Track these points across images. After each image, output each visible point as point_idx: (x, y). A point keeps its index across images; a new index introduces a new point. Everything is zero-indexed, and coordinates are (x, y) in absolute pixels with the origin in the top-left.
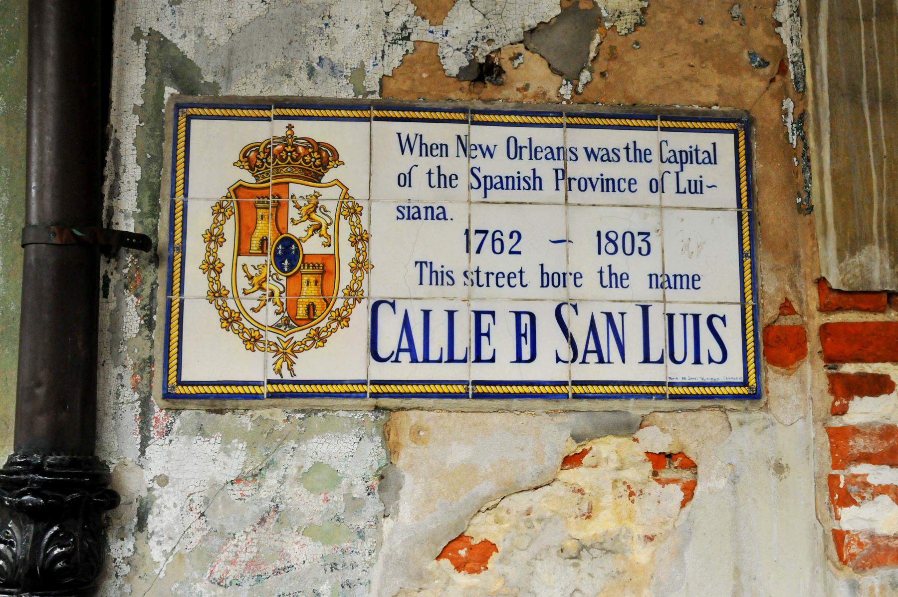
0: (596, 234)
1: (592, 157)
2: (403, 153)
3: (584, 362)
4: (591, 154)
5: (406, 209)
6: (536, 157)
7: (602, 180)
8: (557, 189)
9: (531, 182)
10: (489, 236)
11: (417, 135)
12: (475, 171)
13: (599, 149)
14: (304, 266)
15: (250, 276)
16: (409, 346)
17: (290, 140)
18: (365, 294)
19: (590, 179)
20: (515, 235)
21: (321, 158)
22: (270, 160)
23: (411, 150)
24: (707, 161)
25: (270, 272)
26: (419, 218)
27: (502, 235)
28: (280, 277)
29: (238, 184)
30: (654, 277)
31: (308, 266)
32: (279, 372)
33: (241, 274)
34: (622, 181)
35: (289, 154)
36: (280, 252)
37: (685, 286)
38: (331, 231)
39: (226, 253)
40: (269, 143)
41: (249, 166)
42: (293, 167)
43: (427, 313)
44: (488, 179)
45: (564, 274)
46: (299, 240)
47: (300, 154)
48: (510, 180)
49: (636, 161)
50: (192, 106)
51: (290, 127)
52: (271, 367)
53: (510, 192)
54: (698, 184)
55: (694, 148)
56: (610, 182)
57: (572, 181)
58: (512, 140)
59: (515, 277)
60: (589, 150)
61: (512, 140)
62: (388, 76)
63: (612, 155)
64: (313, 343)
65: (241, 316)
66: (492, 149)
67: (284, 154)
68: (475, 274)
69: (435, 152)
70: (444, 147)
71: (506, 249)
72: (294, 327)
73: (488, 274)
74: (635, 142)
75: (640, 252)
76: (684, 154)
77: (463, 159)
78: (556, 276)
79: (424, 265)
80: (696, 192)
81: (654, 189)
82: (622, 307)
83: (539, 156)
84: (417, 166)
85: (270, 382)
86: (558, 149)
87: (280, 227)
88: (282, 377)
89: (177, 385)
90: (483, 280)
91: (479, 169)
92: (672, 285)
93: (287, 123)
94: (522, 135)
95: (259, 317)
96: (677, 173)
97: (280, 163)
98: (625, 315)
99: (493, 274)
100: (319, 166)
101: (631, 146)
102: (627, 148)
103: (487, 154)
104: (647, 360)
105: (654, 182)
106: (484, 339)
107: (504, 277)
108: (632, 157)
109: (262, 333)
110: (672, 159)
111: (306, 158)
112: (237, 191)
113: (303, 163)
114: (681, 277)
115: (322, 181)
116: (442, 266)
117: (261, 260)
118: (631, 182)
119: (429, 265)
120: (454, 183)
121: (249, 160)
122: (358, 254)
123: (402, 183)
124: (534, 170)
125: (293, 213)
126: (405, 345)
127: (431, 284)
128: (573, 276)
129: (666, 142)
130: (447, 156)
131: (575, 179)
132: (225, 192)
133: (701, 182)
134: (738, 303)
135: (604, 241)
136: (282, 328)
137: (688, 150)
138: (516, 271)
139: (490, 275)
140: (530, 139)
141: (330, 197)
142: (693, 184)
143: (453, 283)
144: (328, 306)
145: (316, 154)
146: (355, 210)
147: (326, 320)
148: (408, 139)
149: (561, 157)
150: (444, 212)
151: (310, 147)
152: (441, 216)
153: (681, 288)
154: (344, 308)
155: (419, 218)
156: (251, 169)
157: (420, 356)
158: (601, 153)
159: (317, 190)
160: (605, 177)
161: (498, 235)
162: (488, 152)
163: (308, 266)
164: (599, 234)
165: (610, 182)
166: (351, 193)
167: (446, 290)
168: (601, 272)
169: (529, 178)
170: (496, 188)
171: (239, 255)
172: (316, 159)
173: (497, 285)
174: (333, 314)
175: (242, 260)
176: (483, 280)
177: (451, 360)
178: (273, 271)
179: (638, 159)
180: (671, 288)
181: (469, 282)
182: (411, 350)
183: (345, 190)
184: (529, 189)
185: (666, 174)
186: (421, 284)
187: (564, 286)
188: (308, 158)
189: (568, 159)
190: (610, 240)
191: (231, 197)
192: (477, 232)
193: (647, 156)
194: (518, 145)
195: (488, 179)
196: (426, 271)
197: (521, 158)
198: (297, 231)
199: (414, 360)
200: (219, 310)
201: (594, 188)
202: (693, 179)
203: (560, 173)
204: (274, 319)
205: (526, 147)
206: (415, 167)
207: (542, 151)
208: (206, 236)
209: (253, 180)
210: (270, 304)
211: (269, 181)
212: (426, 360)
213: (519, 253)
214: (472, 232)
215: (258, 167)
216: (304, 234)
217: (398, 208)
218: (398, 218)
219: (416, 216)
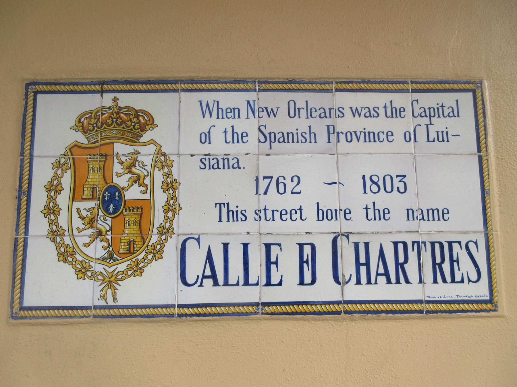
0: (362, 177)
1: (357, 115)
2: (204, 117)
4: (356, 112)
5: (207, 160)
7: (365, 133)
8: (329, 142)
9: (307, 136)
12: (262, 128)
13: (362, 108)
14: (126, 210)
15: (82, 217)
19: (355, 132)
20: (296, 179)
22: (99, 124)
23: (211, 114)
24: (451, 114)
27: (285, 179)
28: (107, 218)
30: (410, 212)
31: (129, 209)
34: (381, 134)
36: (107, 198)
44: (273, 135)
46: (122, 189)
48: (290, 135)
49: (392, 117)
51: (115, 100)
52: (98, 294)
55: (440, 105)
56: (372, 135)
57: (341, 135)
58: (292, 104)
59: (296, 213)
60: (354, 110)
61: (292, 104)
63: (372, 112)
67: (110, 121)
68: (263, 212)
69: (229, 115)
70: (236, 111)
71: (289, 190)
72: (118, 260)
73: (273, 211)
74: (391, 102)
75: (399, 191)
76: (432, 110)
78: (329, 212)
79: (222, 205)
80: (443, 141)
81: (408, 139)
83: (314, 114)
84: (214, 126)
90: (269, 215)
91: (265, 127)
93: (112, 95)
94: (300, 98)
95: (89, 251)
96: (427, 126)
97: (107, 127)
99: (277, 211)
100: (138, 129)
101: (389, 105)
102: (385, 107)
105: (407, 134)
108: (389, 113)
109: (92, 264)
110: (423, 114)
112: (72, 150)
113: (125, 127)
114: (433, 210)
116: (237, 207)
117: (91, 204)
118: (389, 134)
119: (226, 205)
120: (245, 139)
123: (203, 141)
124: (310, 127)
125: (117, 168)
127: (228, 221)
129: (417, 101)
130: (239, 117)
131: (343, 133)
133: (447, 132)
135: (368, 183)
136: (108, 261)
137: (436, 106)
139: (275, 212)
147: (144, 253)
148: (208, 105)
154: (158, 242)
155: (218, 168)
156: (85, 131)
158: (364, 112)
159: (136, 148)
160: (367, 131)
161: (281, 180)
162: (272, 113)
163: (129, 209)
164: (364, 177)
165: (372, 135)
166: (164, 150)
168: (366, 208)
169: (306, 134)
170: (279, 142)
171: (73, 200)
173: (281, 219)
174: (150, 248)
176: (269, 215)
178: (101, 213)
185: (418, 128)
186: (220, 220)
187: (336, 219)
192: (265, 178)
194: (297, 107)
195: (273, 135)
196: (224, 210)
197: (299, 117)
198: (121, 181)
201: (358, 140)
202: (440, 131)
203: (331, 128)
204: (101, 253)
205: (304, 109)
206: (213, 127)
207: (316, 111)
209: (86, 142)
218: (200, 168)
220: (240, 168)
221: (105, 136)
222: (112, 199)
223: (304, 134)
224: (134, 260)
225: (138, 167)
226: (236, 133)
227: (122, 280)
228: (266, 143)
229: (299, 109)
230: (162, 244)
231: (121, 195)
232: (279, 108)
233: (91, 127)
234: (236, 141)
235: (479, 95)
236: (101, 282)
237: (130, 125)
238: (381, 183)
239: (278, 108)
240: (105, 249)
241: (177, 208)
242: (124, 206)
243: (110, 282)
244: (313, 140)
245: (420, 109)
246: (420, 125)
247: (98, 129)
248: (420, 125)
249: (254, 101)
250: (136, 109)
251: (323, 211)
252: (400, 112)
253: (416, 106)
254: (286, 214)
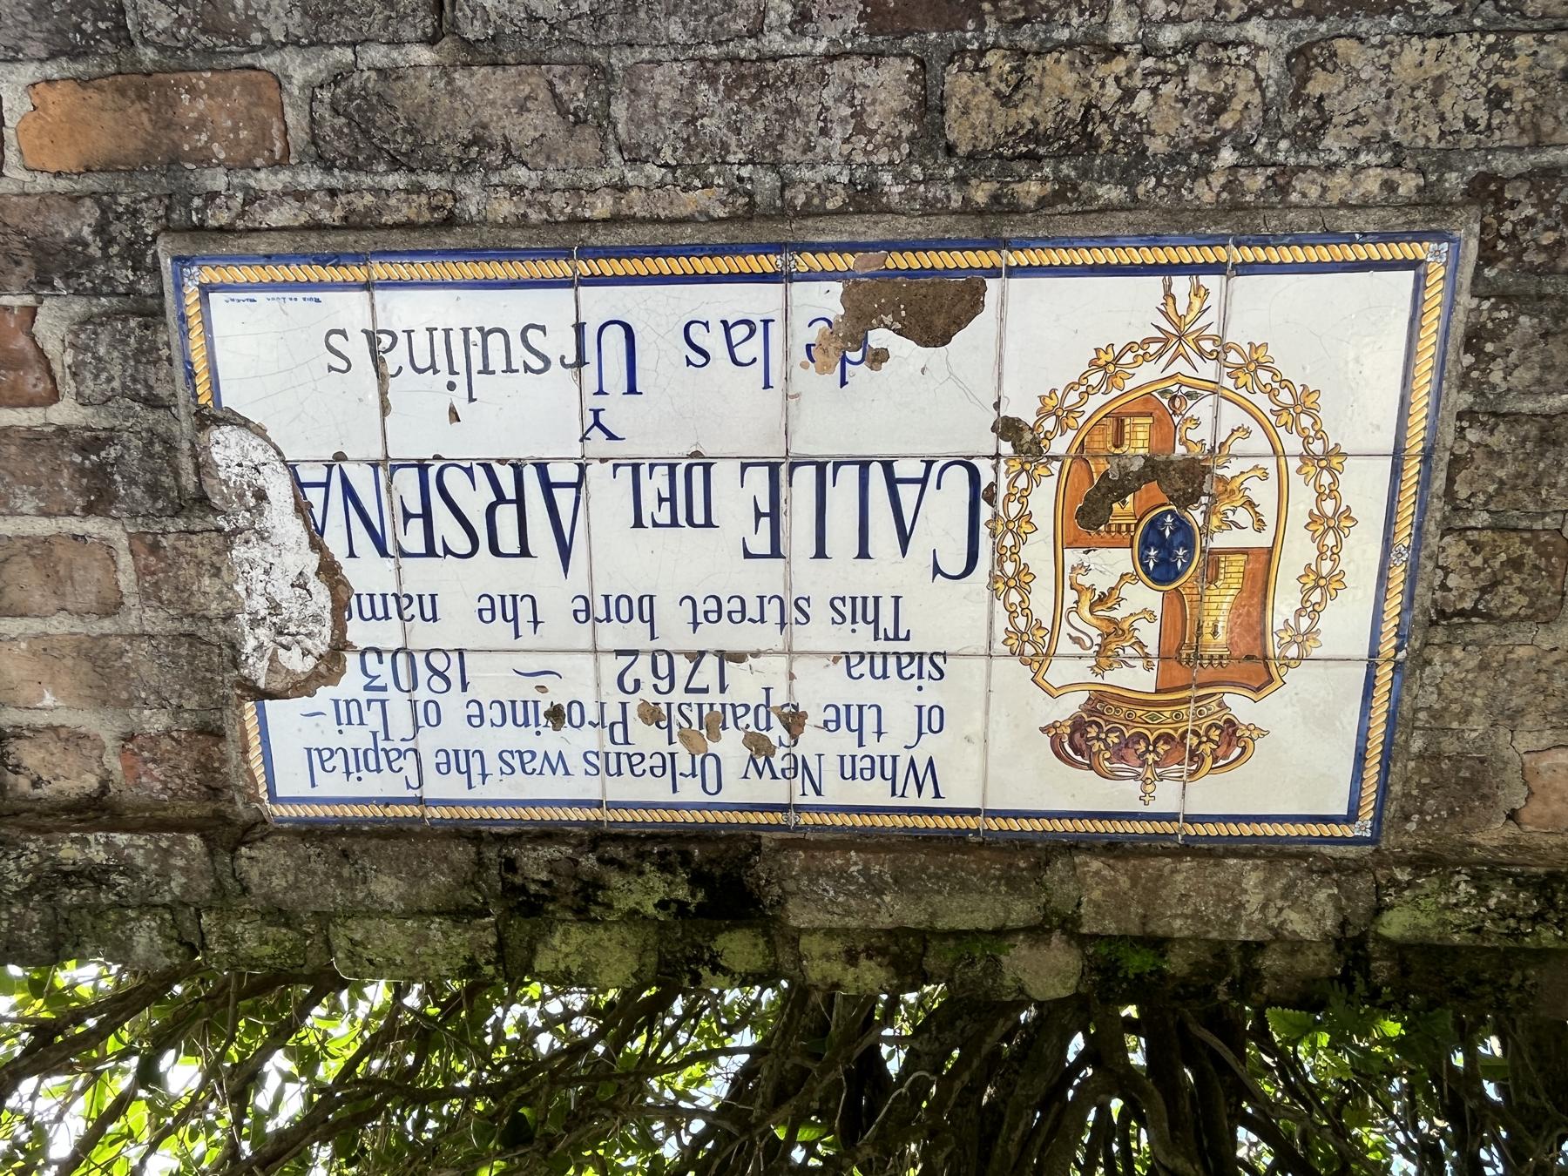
14: (1128, 530)
17: (1149, 775)
31: (1119, 532)
39: (1298, 552)
46: (1137, 578)
52: (1213, 300)
60: (561, 769)
65: (1273, 419)
83: (657, 761)
93: (1153, 808)
95: (1232, 416)
101: (476, 779)
102: (484, 776)
109: (1228, 383)
117: (1220, 541)
125: (1149, 634)
132: (1291, 676)
136: (1185, 390)
141: (1070, 669)
158: (537, 764)
159: (1099, 679)
171: (1270, 551)
172: (1098, 739)
175: (1264, 540)
194: (699, 778)
198: (1144, 598)
207: (652, 768)
209: (1227, 699)
215: (1218, 727)
216: (1127, 590)
227: (1149, 341)
231: (1142, 564)
240: (1191, 418)
252: (448, 763)
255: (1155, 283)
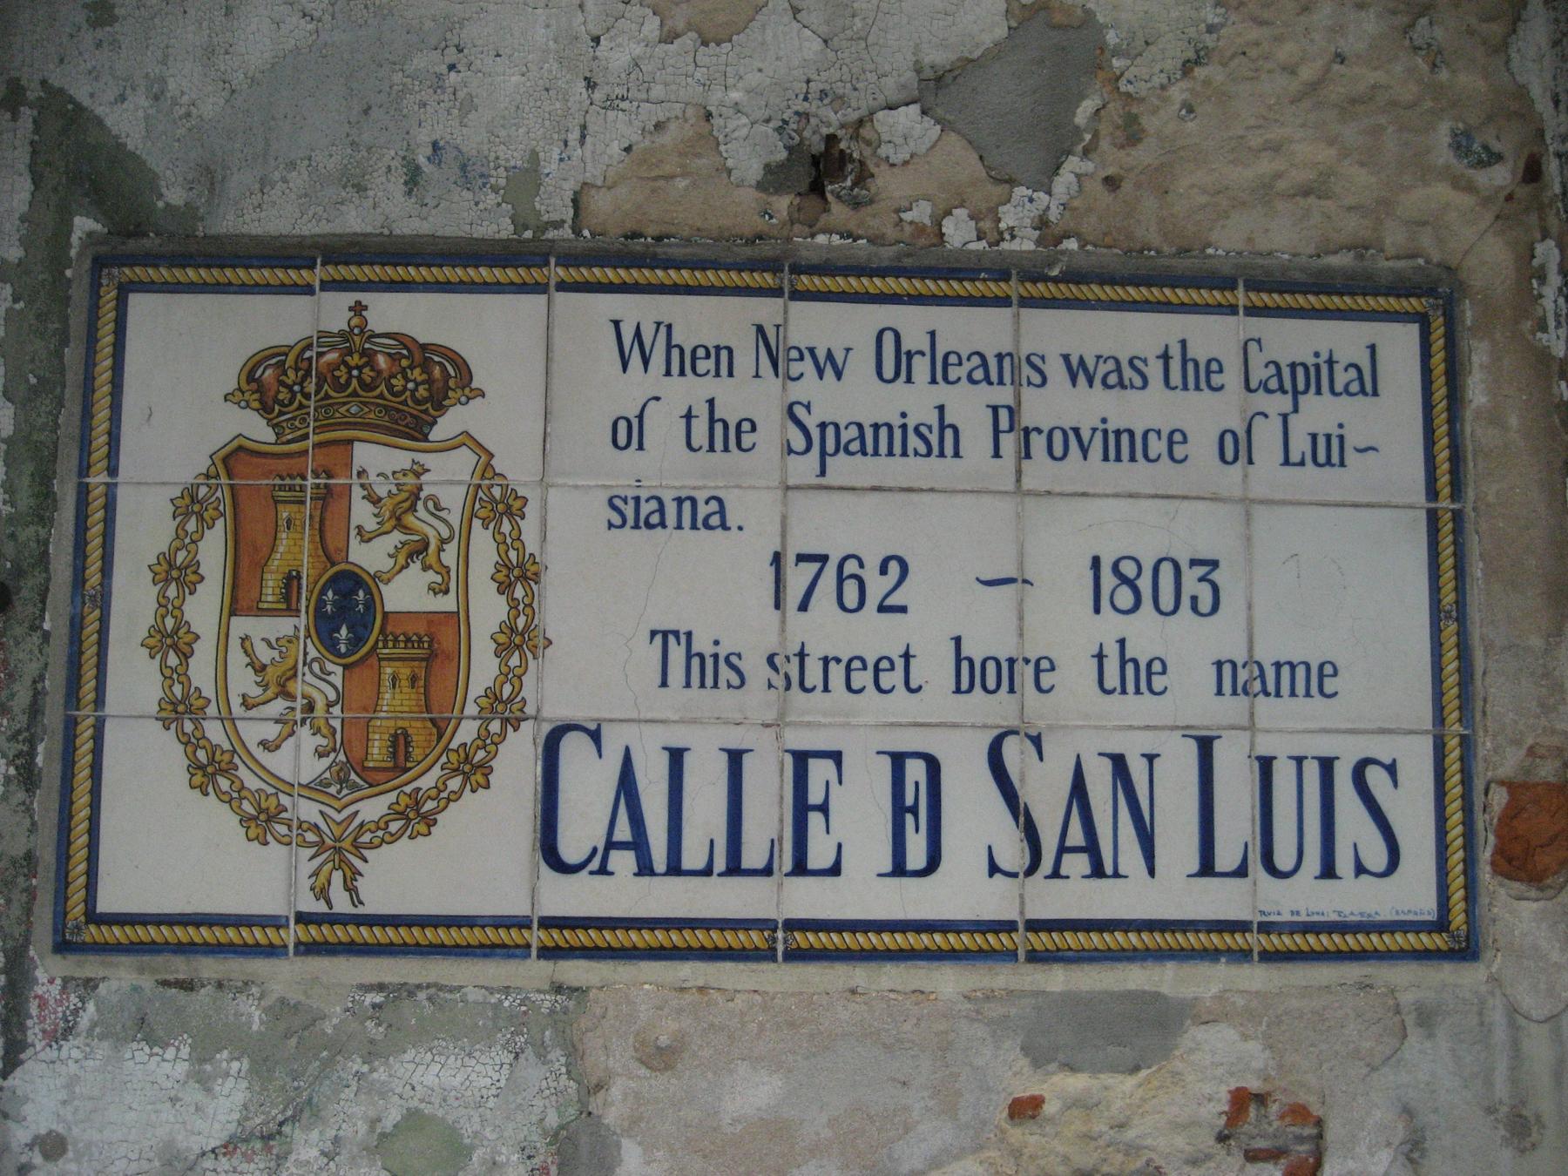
0: (1089, 563)
1: (1082, 378)
2: (625, 369)
3: (1056, 874)
4: (1077, 370)
5: (631, 503)
6: (945, 379)
7: (1105, 432)
8: (997, 455)
9: (934, 439)
10: (831, 570)
11: (658, 324)
12: (800, 412)
13: (1098, 357)
14: (385, 642)
16: (633, 836)
18: (530, 710)
19: (1076, 431)
20: (894, 567)
21: (430, 381)
22: (311, 387)
23: (646, 362)
24: (1355, 387)
25: (306, 654)
26: (663, 524)
27: (861, 565)
28: (330, 667)
29: (235, 444)
30: (1227, 669)
31: (396, 640)
32: (322, 893)
33: (237, 658)
34: (1152, 437)
35: (355, 373)
36: (329, 608)
37: (1300, 689)
38: (450, 556)
39: (203, 609)
40: (309, 347)
41: (261, 401)
42: (365, 404)
43: (676, 757)
44: (830, 431)
45: (1011, 661)
47: (379, 372)
48: (883, 432)
49: (1185, 388)
50: (132, 260)
51: (359, 308)
53: (883, 461)
54: (1335, 443)
55: (1324, 356)
56: (1125, 438)
57: (1034, 436)
58: (888, 339)
59: (892, 668)
60: (1075, 362)
61: (888, 339)
62: (593, 186)
63: (1128, 373)
64: (406, 827)
65: (236, 760)
66: (839, 357)
67: (342, 373)
68: (795, 661)
69: (703, 366)
70: (724, 354)
72: (357, 788)
73: (826, 661)
74: (1183, 343)
75: (1195, 608)
76: (1300, 372)
77: (771, 383)
78: (991, 666)
79: (671, 639)
80: (1329, 462)
81: (1229, 455)
82: (1148, 742)
83: (953, 373)
84: (657, 399)
85: (303, 919)
86: (1000, 357)
87: (331, 547)
88: (329, 903)
89: (87, 923)
90: (814, 675)
91: (808, 407)
92: (1271, 688)
93: (349, 298)
94: (913, 323)
95: (280, 763)
96: (1285, 417)
98: (1156, 762)
99: (838, 661)
101: (1175, 351)
103: (829, 372)
104: (1207, 868)
106: (815, 819)
107: (865, 668)
108: (1175, 377)
109: (285, 800)
111: (394, 381)
114: (1293, 666)
115: (431, 437)
116: (716, 643)
118: (1177, 437)
119: (683, 639)
120: (747, 440)
121: (260, 388)
122: (513, 612)
123: (622, 440)
124: (941, 408)
125: (362, 514)
126: (623, 832)
127: (688, 685)
128: (1032, 665)
129: (1259, 341)
130: (731, 374)
131: (1039, 431)
132: (203, 464)
133: (1341, 438)
134: (1426, 732)
135: (1108, 580)
136: (333, 790)
137: (1311, 361)
138: (895, 653)
139: (832, 665)
140: (933, 334)
142: (1321, 442)
143: (743, 683)
144: (440, 737)
145: (417, 371)
146: (509, 507)
147: (436, 772)
148: (638, 334)
149: (1007, 378)
150: (722, 512)
151: (404, 357)
152: (715, 520)
153: (1293, 694)
154: (479, 742)
155: (663, 524)
157: (659, 859)
158: (1103, 368)
160: (1111, 427)
161: (851, 567)
162: (831, 365)
163: (396, 640)
164: (1096, 562)
165: (1125, 438)
167: (724, 700)
168: (1100, 657)
169: (930, 428)
173: (849, 687)
174: (453, 757)
176: (814, 675)
177: (734, 868)
178: (313, 653)
179: (1191, 384)
180: (1267, 694)
181: (779, 681)
182: (639, 844)
183: (484, 458)
184: (929, 454)
185: (1258, 420)
186: (664, 684)
187: (1012, 690)
188: (398, 382)
189: (1024, 381)
190: (1125, 580)
191: (217, 476)
192: (801, 558)
193: (1213, 376)
194: (904, 349)
195: (830, 431)
196: (677, 653)
197: (909, 380)
198: (369, 556)
199: (645, 868)
200: (186, 744)
201: (1085, 452)
202: (1321, 431)
203: (1004, 415)
205: (923, 354)
207: (960, 364)
208: (157, 568)
209: (268, 435)
210: (304, 732)
211: (305, 437)
212: (675, 869)
213: (903, 609)
214: (790, 559)
215: (282, 404)
217: (610, 501)
218: (611, 525)
219: (655, 519)
220: (729, 529)
221: (327, 418)
222: (344, 609)
223: (923, 429)
224: (408, 789)
225: (421, 512)
226: (719, 420)
227: (371, 846)
228: (809, 454)
229: (910, 355)
230: (491, 743)
232: (851, 352)
233: (284, 395)
234: (719, 444)
235: (1438, 331)
236: (313, 851)
237: (399, 388)
238: (1145, 584)
239: (848, 350)
241: (541, 642)
242: (382, 630)
243: (338, 850)
244: (949, 449)
245: (1266, 366)
246: (1266, 416)
247: (305, 402)
248: (1266, 416)
249: (778, 326)
250: (421, 341)
251: (971, 661)
253: (1257, 360)
254: (865, 668)
255: (369, 908)
